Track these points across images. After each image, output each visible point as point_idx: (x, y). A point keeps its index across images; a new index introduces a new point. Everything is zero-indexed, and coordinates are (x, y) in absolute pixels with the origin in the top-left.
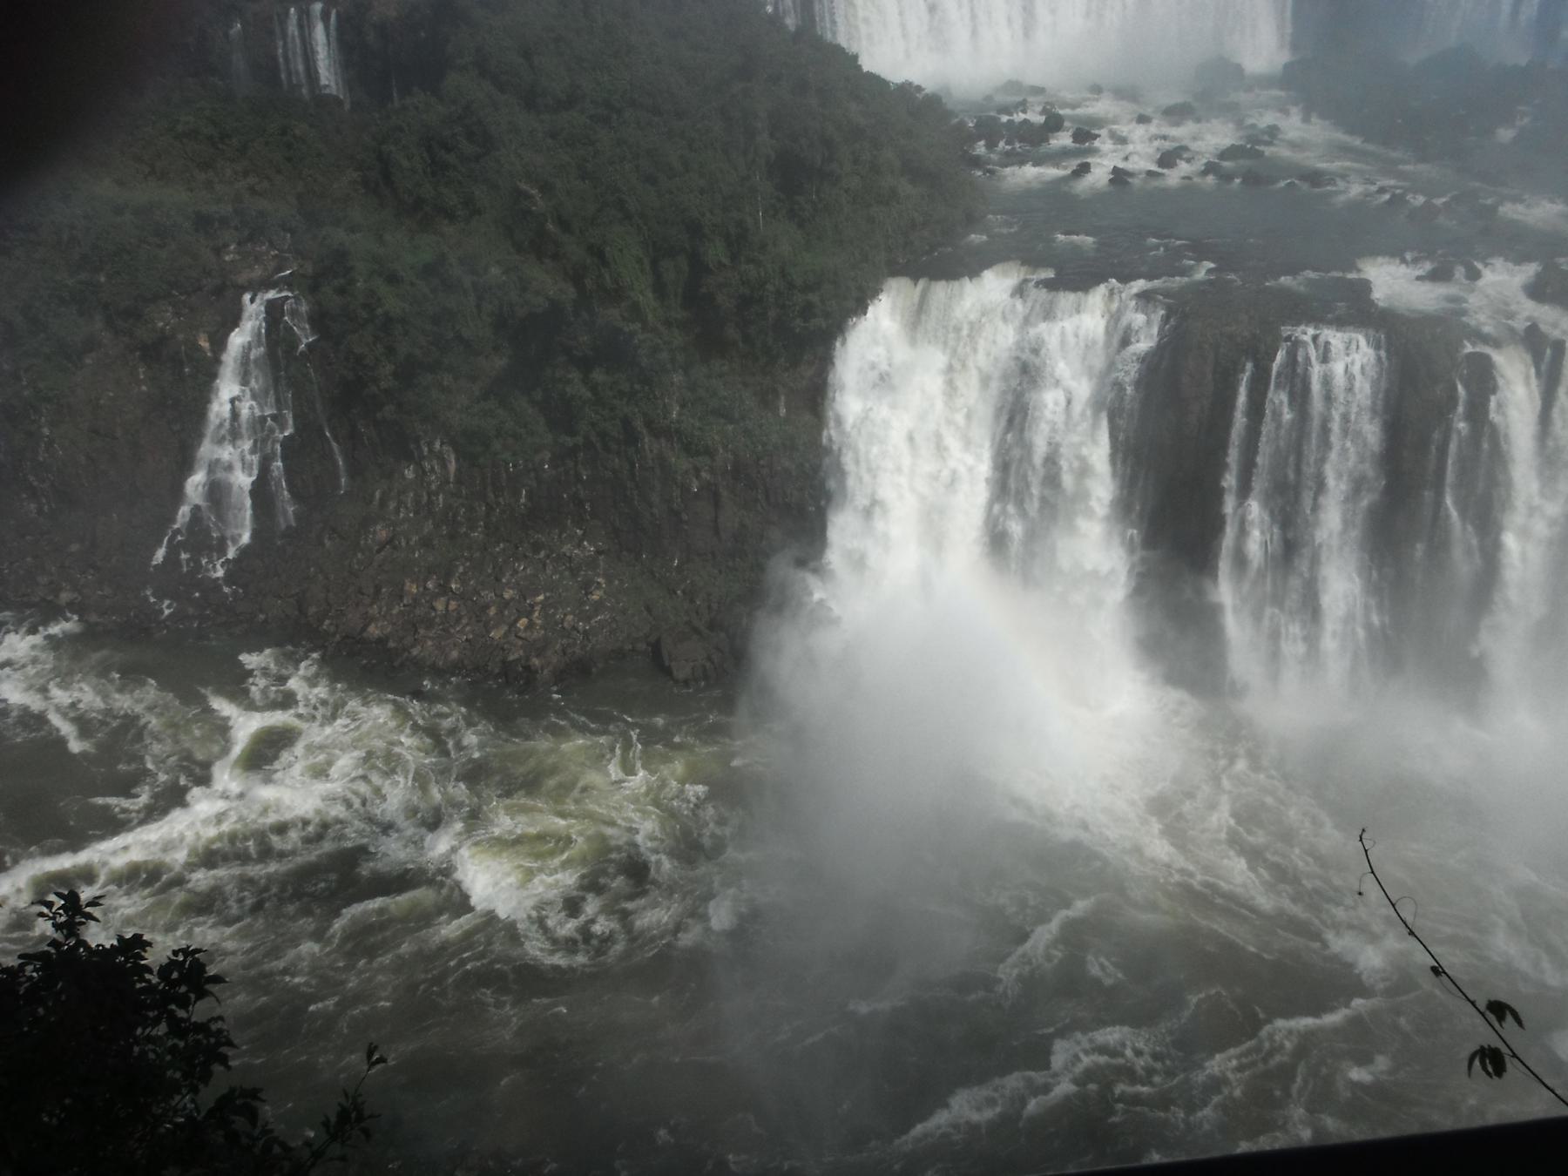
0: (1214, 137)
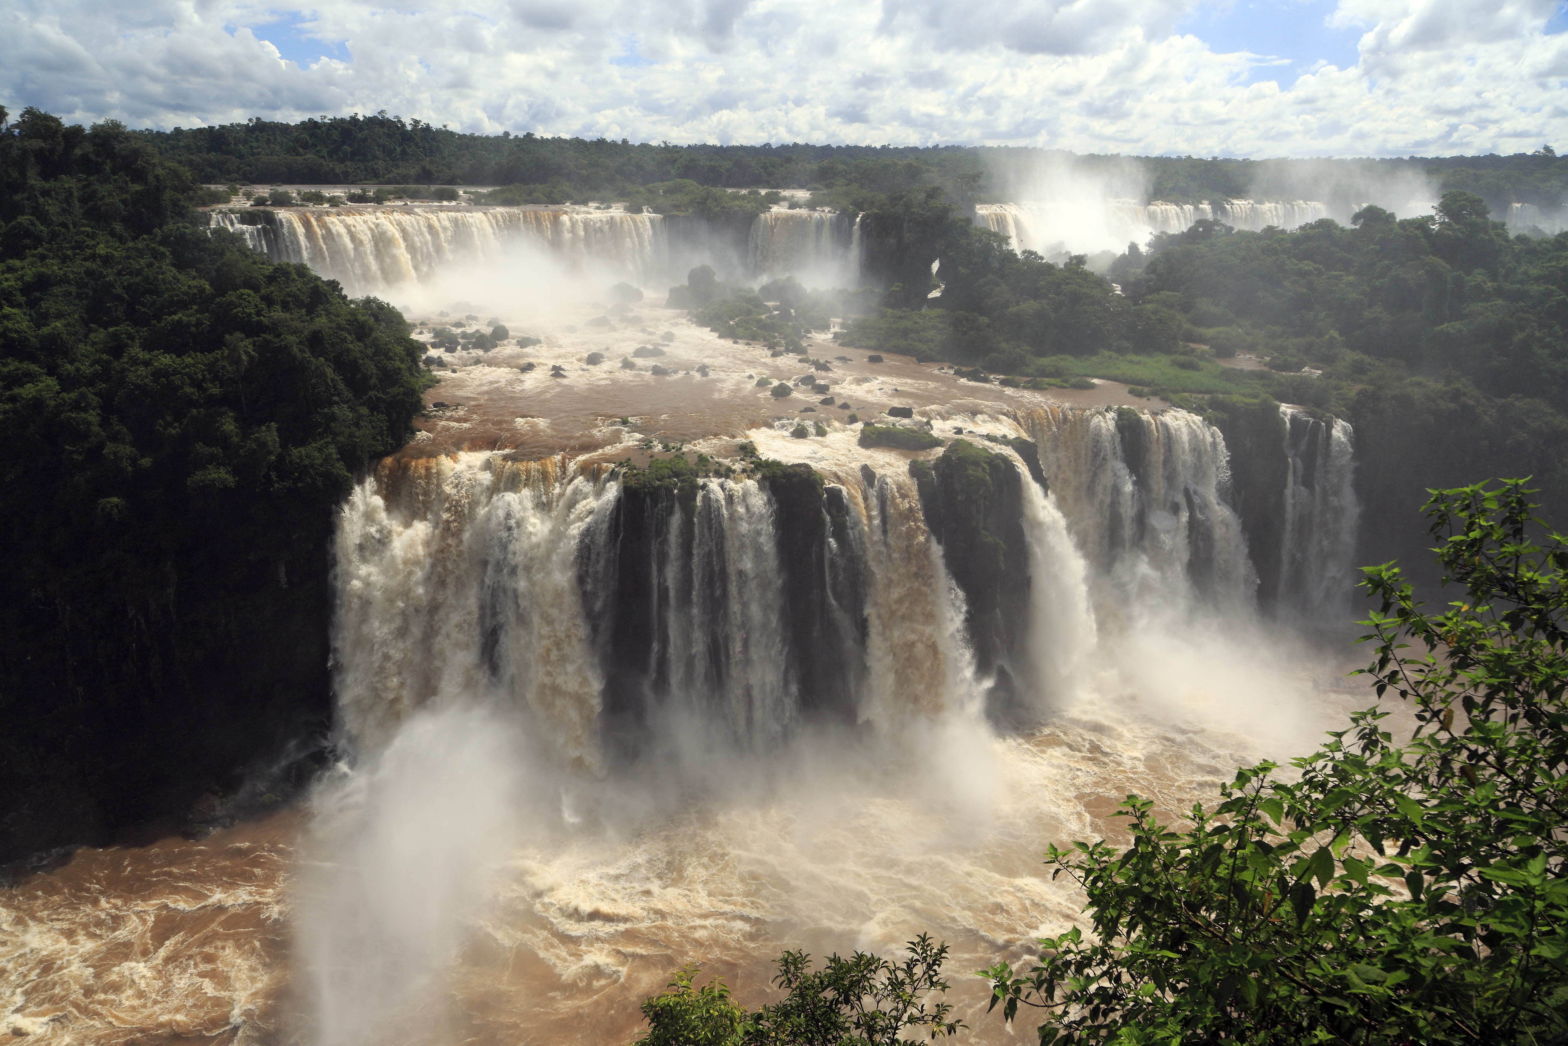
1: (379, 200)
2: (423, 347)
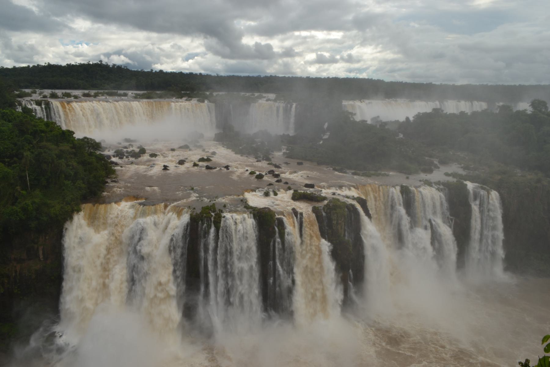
0: (195, 155)
1: (96, 96)
2: (109, 157)
